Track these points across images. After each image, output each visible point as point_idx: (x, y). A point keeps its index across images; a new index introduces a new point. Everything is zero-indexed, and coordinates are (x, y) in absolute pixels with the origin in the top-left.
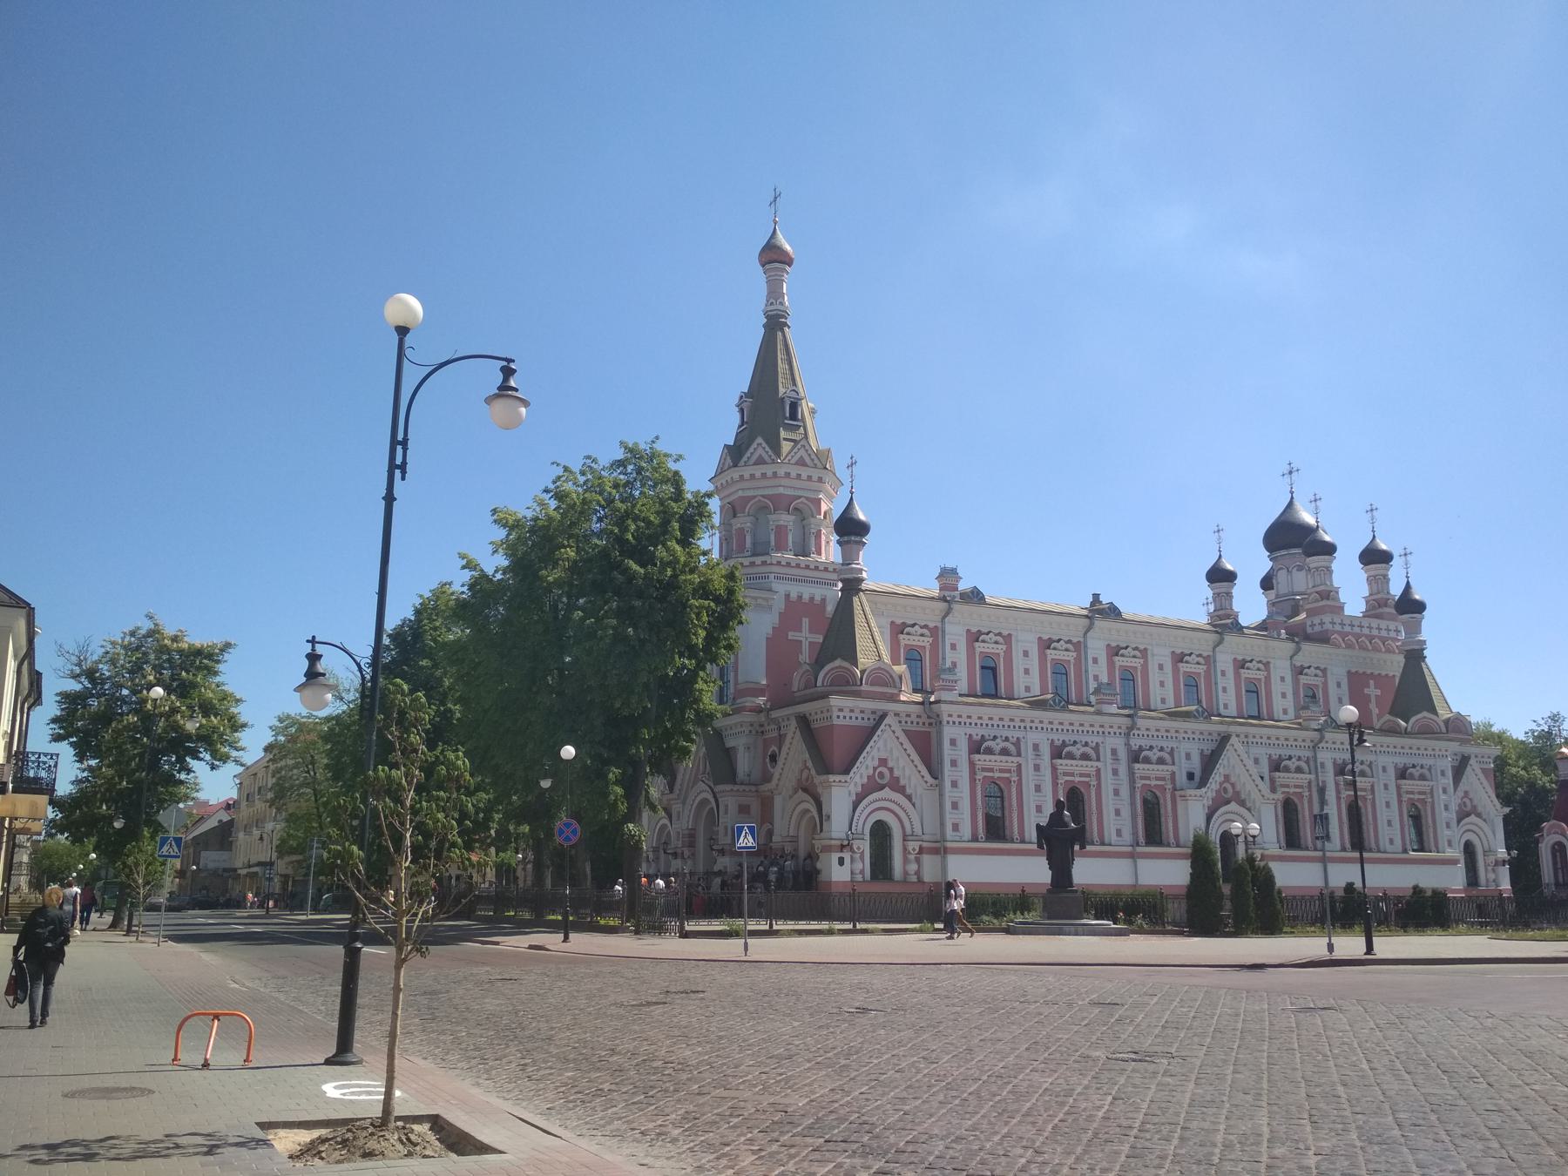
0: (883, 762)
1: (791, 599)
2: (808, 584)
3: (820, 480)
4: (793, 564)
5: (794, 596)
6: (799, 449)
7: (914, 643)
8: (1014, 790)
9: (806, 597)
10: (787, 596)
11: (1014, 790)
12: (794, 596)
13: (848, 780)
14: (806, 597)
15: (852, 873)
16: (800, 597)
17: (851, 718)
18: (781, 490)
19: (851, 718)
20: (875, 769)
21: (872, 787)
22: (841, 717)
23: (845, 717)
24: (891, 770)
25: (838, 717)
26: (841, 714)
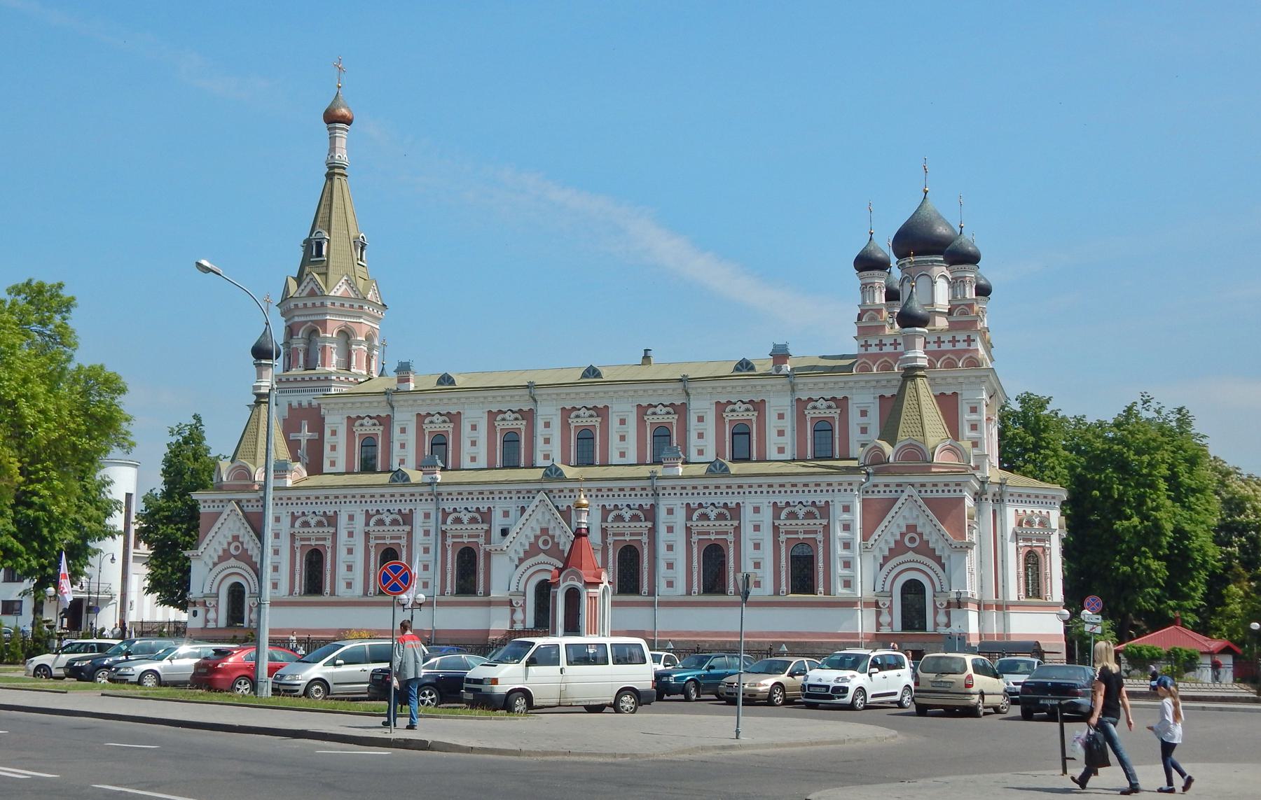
0: (236, 538)
1: (293, 407)
2: (300, 394)
3: (322, 304)
4: (284, 380)
5: (295, 404)
6: (308, 283)
7: (370, 432)
8: (329, 555)
9: (305, 404)
10: (290, 405)
11: (329, 555)
12: (295, 404)
13: (200, 554)
14: (305, 404)
15: (207, 621)
16: (300, 404)
17: (214, 507)
18: (296, 319)
19: (214, 507)
20: (229, 544)
21: (225, 556)
22: (207, 507)
23: (209, 507)
24: (242, 543)
25: (204, 507)
26: (206, 505)
